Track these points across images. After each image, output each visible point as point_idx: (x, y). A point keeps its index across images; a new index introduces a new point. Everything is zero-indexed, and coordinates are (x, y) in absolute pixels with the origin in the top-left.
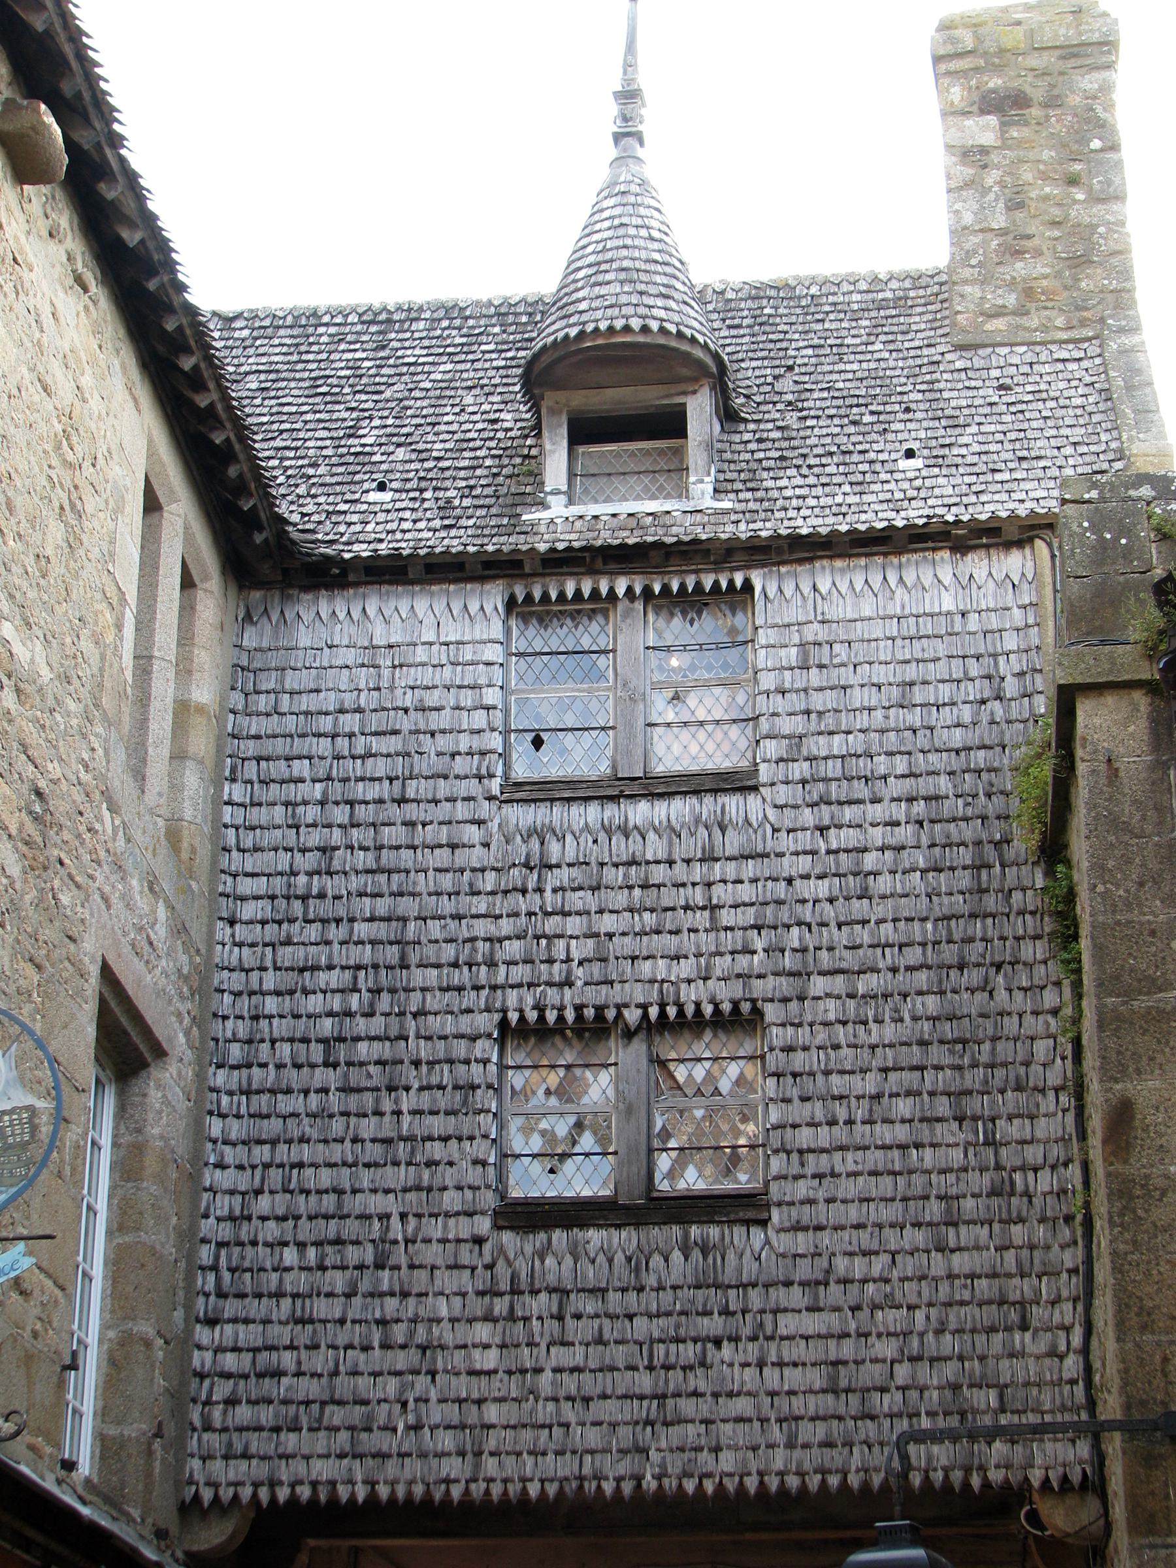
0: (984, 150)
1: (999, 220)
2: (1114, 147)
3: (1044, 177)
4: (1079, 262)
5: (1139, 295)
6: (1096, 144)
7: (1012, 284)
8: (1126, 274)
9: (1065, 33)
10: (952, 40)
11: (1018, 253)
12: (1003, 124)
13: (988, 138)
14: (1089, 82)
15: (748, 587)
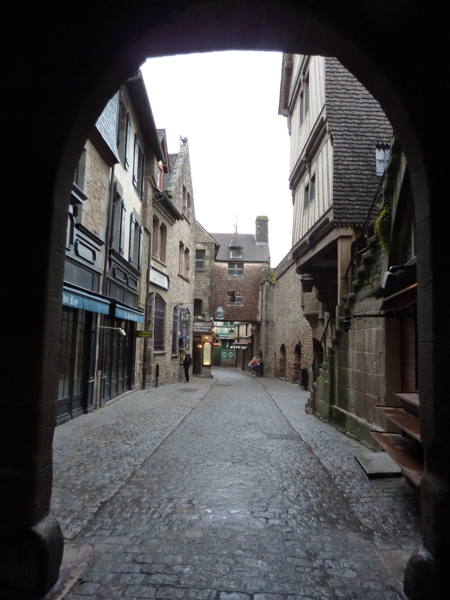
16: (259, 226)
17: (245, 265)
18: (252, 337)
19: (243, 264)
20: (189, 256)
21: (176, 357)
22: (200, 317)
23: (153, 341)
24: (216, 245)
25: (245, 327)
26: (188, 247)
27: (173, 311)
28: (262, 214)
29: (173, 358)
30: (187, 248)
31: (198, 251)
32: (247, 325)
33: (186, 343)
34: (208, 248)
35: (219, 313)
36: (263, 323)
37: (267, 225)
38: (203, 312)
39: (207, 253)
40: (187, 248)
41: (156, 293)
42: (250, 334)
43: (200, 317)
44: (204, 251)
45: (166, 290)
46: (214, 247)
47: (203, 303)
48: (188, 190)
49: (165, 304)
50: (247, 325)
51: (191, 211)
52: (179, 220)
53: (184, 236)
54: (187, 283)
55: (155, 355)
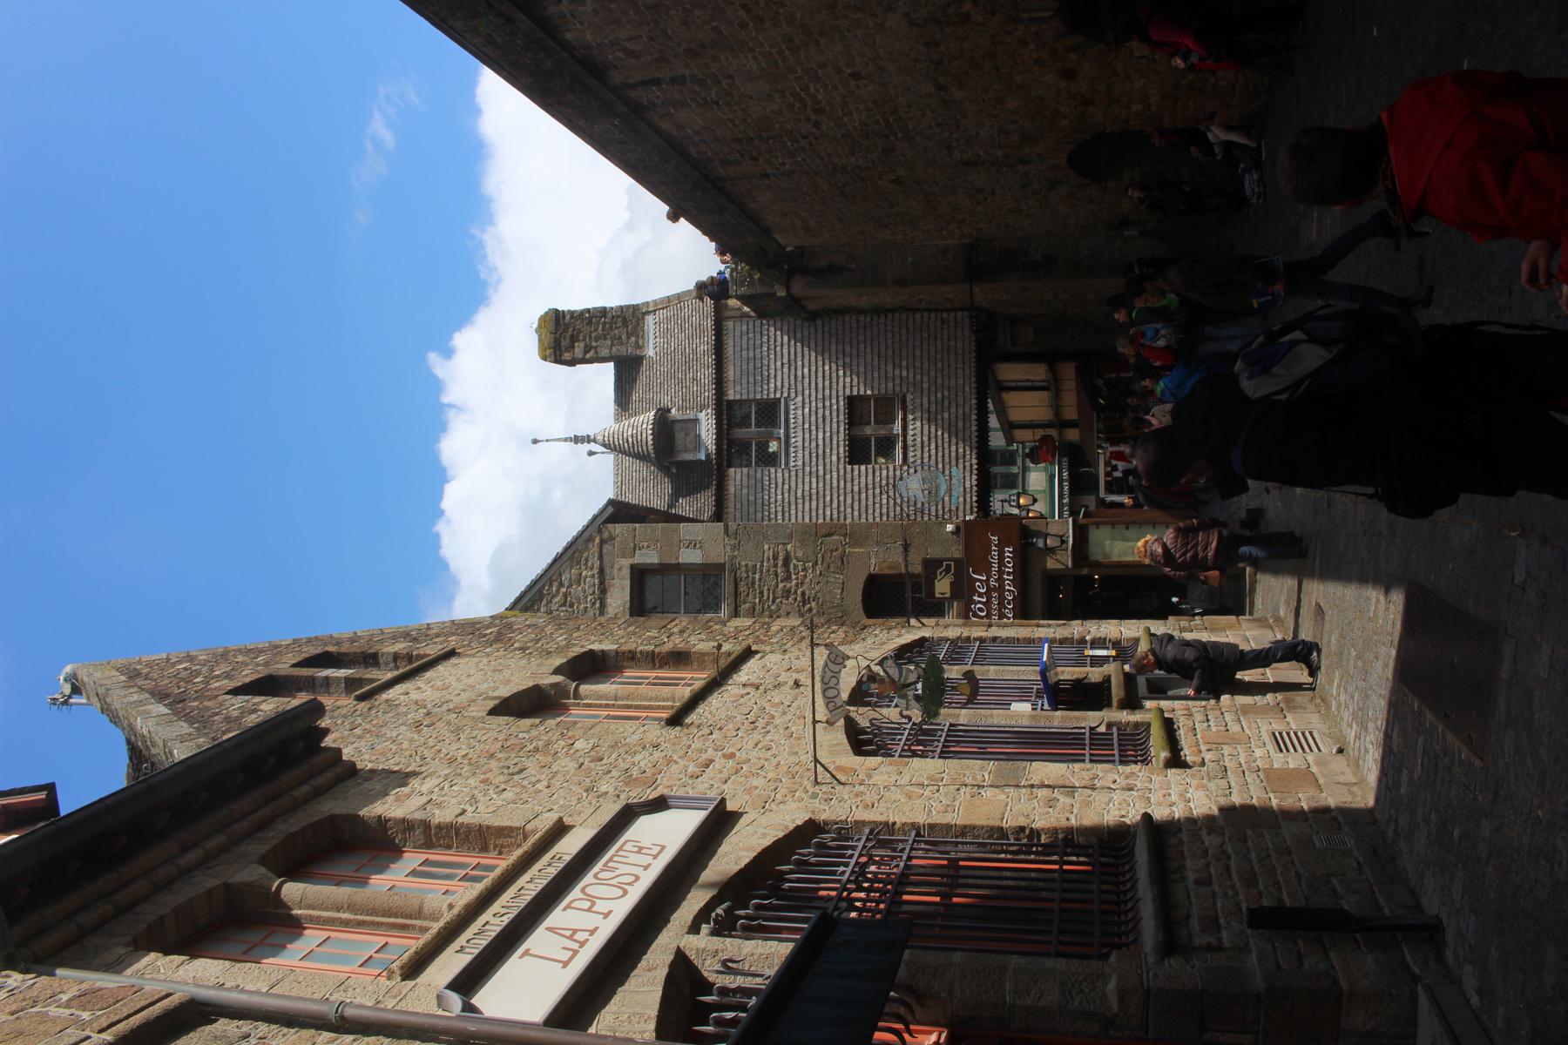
0: (586, 346)
1: (609, 342)
2: (588, 310)
3: (596, 330)
4: (625, 321)
5: (635, 303)
6: (587, 315)
7: (629, 338)
8: (628, 307)
9: (553, 324)
10: (550, 354)
11: (620, 337)
12: (578, 341)
13: (582, 345)
14: (568, 317)
15: (727, 401)
16: (579, 349)
17: (732, 394)
18: (1051, 358)
19: (729, 402)
20: (617, 652)
21: (1169, 726)
22: (942, 587)
23: (1061, 964)
24: (613, 519)
25: (1011, 398)
26: (558, 661)
27: (873, 761)
28: (529, 343)
29: (1176, 761)
30: (557, 671)
31: (639, 607)
32: (1003, 388)
33: (1080, 662)
34: (623, 556)
35: (932, 493)
36: (983, 295)
37: (572, 313)
38: (917, 568)
39: (650, 557)
40: (557, 671)
41: (694, 928)
42: (1038, 372)
43: (942, 587)
44: (640, 575)
45: (720, 822)
46: (618, 529)
47: (886, 572)
48: (283, 667)
49: (809, 831)
50: (1003, 388)
51: (400, 646)
52: (326, 732)
53: (484, 687)
54: (752, 664)
55: (1171, 945)
